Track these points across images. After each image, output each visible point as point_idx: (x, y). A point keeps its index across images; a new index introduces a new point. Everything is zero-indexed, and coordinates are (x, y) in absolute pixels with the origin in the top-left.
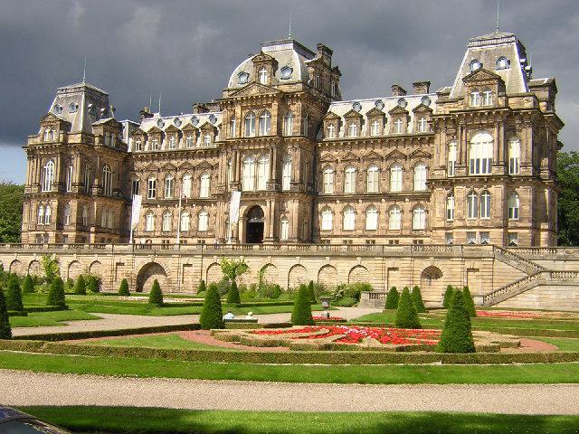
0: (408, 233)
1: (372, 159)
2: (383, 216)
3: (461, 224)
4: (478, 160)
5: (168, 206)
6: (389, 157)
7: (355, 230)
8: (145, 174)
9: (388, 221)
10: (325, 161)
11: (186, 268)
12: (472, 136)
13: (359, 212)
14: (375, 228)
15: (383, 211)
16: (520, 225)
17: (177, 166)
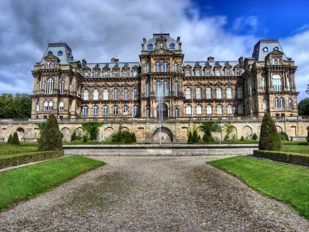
0: (226, 115)
1: (210, 85)
2: (214, 109)
3: (273, 110)
4: (276, 86)
7: (202, 114)
9: (216, 111)
12: (273, 75)
14: (211, 113)
16: (294, 111)
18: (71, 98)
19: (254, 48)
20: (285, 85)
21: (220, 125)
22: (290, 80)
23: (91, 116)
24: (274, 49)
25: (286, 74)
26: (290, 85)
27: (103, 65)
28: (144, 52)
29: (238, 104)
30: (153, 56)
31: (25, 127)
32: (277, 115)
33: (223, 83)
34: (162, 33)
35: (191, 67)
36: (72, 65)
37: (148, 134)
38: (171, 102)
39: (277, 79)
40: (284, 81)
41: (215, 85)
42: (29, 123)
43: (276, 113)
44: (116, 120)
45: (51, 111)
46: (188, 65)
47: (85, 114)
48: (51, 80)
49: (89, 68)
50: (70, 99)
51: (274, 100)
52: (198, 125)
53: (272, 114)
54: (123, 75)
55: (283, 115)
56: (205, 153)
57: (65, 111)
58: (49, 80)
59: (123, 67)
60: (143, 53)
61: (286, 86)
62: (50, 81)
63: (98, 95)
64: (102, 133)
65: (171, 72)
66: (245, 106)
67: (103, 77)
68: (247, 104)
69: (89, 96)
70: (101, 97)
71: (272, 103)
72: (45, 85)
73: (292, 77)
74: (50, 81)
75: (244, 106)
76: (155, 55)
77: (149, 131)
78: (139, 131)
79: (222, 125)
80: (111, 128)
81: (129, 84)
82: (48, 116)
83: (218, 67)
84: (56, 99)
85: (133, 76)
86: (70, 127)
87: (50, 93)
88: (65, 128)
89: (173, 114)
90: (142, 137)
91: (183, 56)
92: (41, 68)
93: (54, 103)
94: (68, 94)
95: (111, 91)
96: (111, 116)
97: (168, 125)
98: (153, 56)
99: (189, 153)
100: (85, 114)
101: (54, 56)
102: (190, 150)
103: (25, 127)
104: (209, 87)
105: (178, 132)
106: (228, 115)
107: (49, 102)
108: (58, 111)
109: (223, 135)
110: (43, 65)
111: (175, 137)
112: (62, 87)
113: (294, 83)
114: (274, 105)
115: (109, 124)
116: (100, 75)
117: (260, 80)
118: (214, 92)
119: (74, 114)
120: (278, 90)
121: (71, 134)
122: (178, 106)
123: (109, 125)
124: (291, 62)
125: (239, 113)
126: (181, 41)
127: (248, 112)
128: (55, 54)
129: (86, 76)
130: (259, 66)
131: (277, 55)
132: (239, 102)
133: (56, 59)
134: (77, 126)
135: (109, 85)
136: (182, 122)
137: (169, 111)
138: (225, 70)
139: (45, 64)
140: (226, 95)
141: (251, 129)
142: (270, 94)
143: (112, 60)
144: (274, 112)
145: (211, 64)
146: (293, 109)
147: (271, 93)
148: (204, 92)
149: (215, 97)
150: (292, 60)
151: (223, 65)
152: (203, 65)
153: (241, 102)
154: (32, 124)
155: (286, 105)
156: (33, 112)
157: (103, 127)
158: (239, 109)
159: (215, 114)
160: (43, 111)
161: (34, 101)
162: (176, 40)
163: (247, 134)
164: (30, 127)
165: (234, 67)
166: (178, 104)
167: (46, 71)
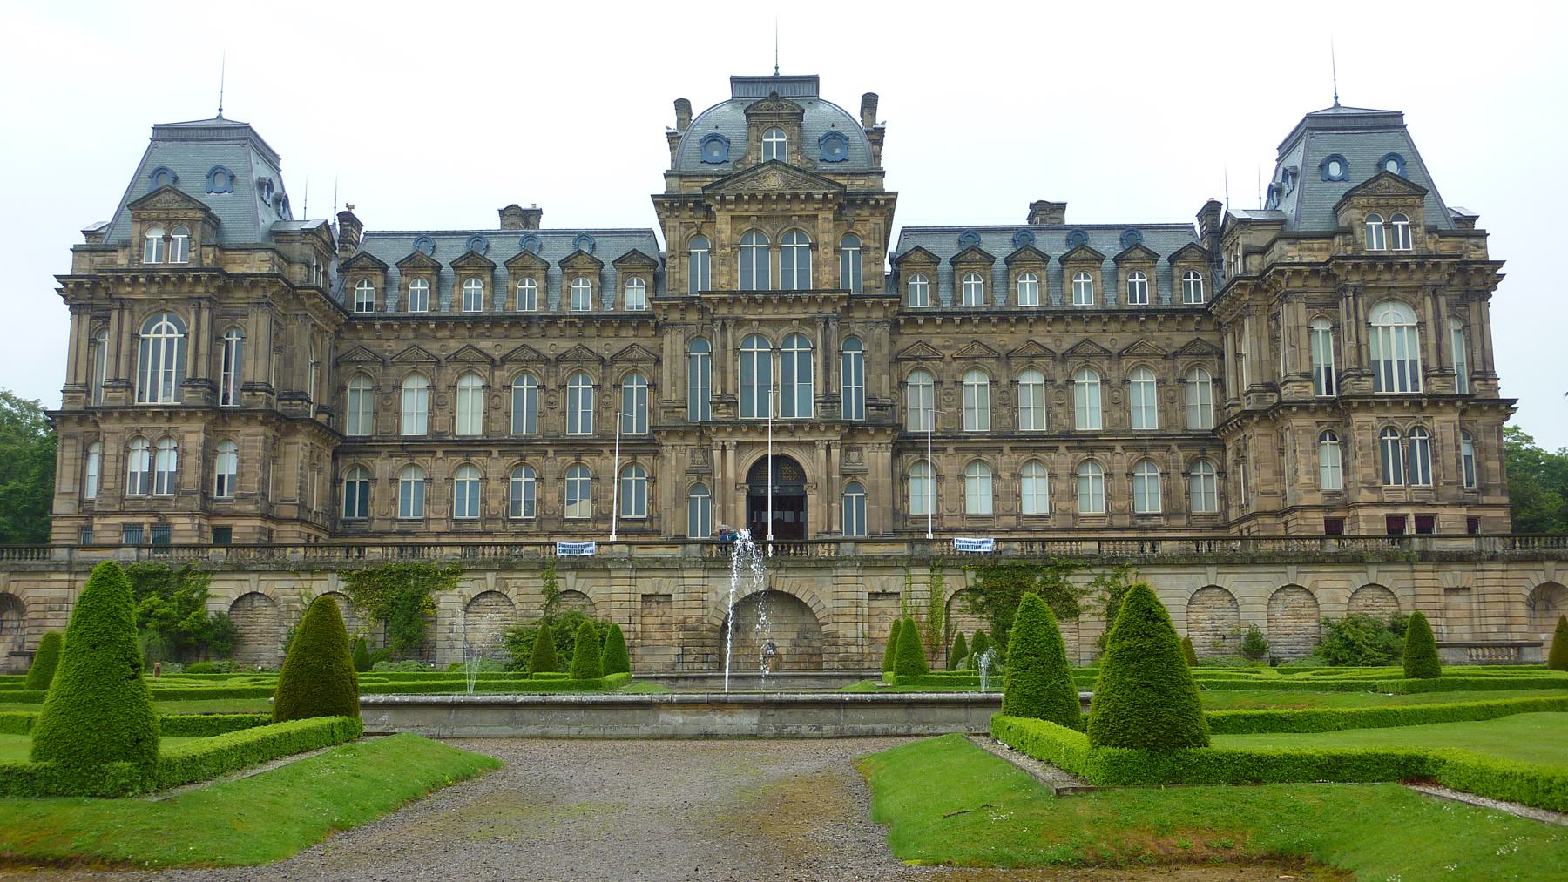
0: (1126, 522)
1: (1032, 358)
2: (1062, 486)
3: (1374, 497)
4: (1388, 364)
5: (469, 454)
6: (1072, 352)
7: (996, 516)
8: (393, 371)
9: (1074, 496)
10: (916, 358)
11: (875, 604)
12: (1369, 307)
13: (1005, 475)
14: (1045, 511)
15: (1062, 472)
16: (1486, 500)
17: (497, 355)
18: (277, 430)
19: (1276, 155)
20: (1433, 364)
21: (1070, 579)
22: (1467, 327)
23: (386, 526)
24: (1380, 165)
25: (1442, 300)
26: (1471, 363)
27: (454, 242)
28: (681, 176)
29: (1192, 463)
30: (731, 202)
31: (30, 593)
32: (1395, 524)
33: (1106, 345)
34: (782, 73)
35: (936, 260)
36: (282, 248)
37: (694, 629)
38: (823, 453)
39: (1393, 330)
40: (1432, 341)
41: (1065, 357)
42: (52, 568)
43: (1390, 512)
44: (527, 552)
45: (165, 499)
46: (918, 248)
47: (350, 510)
48: (170, 331)
49: (380, 262)
50: (270, 432)
51: (1378, 444)
52: (952, 583)
53: (1369, 519)
54: (565, 301)
55: (1425, 525)
56: (893, 729)
57: (245, 497)
58: (159, 331)
59: (567, 259)
60: (676, 182)
61: (1441, 369)
62: (164, 335)
63: (424, 408)
64: (452, 624)
65: (827, 287)
66: (1230, 471)
67: (455, 312)
68: (1237, 463)
69: (376, 412)
70: (441, 422)
71: (1364, 456)
72: (132, 353)
73: (1474, 320)
74: (164, 335)
75: (1222, 473)
76: (739, 197)
77: (699, 612)
78: (646, 612)
79: (1078, 580)
80: (499, 594)
81: (600, 351)
82: (146, 527)
83: (1082, 261)
84: (194, 433)
85: (623, 304)
86: (280, 592)
87: (160, 402)
88: (252, 594)
89: (835, 518)
90: (661, 643)
91: (892, 198)
92: (112, 262)
93: (181, 454)
94: (262, 407)
95: (497, 386)
96: (499, 526)
97: (798, 581)
98: (731, 202)
99: (828, 729)
100: (350, 510)
101: (188, 199)
102: (832, 714)
103: (30, 593)
104: (1031, 367)
105: (847, 618)
106: (1139, 522)
107: (153, 450)
108: (206, 496)
109: (1090, 633)
110: (126, 245)
111: (836, 645)
112: (227, 368)
113: (1486, 347)
114: (1377, 470)
115: (490, 577)
116: (438, 298)
117: (1304, 332)
118: (1061, 394)
119: (295, 517)
120: (1397, 391)
121: (282, 630)
122: (865, 472)
123: (490, 580)
124: (1468, 236)
125: (1195, 512)
126: (880, 117)
127: (1241, 507)
128: (193, 186)
129: (360, 305)
130: (1297, 260)
131: (1392, 202)
132: (1195, 452)
133: (200, 215)
134: (319, 587)
135: (489, 352)
136: (869, 564)
137: (812, 499)
138: (1122, 277)
139: (136, 240)
140: (1127, 409)
141: (1233, 600)
142: (1355, 410)
143: (502, 212)
144: (1380, 504)
145: (1043, 242)
146: (1484, 490)
147: (1360, 403)
148: (1005, 396)
149: (1066, 422)
150: (1478, 225)
151: (1109, 247)
152: (1001, 249)
153: (1210, 452)
154: (70, 573)
155: (1444, 468)
156: (60, 506)
157: (456, 591)
158: (1193, 490)
159: (1064, 513)
160: (123, 499)
161: (68, 442)
162: (855, 110)
163: (1214, 630)
164: (58, 592)
165: (1172, 259)
166: (860, 460)
167: (141, 280)
